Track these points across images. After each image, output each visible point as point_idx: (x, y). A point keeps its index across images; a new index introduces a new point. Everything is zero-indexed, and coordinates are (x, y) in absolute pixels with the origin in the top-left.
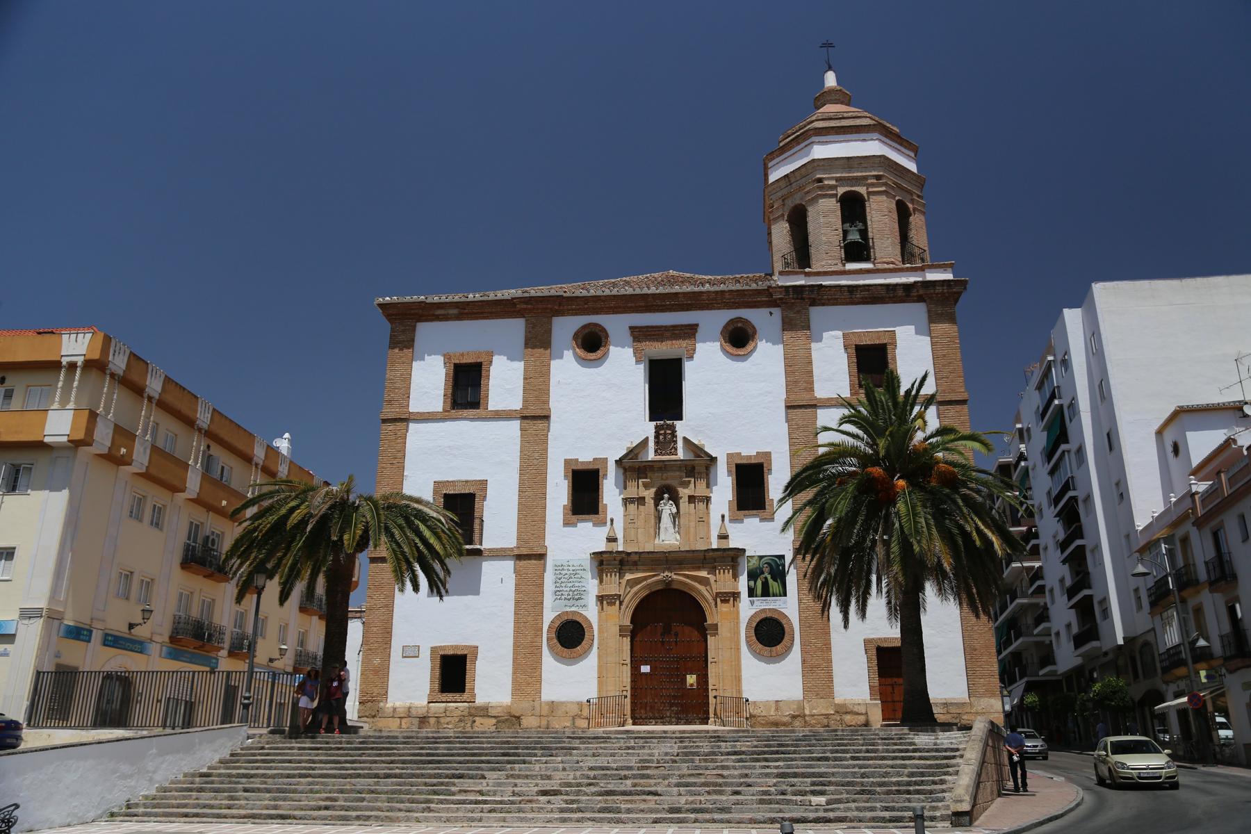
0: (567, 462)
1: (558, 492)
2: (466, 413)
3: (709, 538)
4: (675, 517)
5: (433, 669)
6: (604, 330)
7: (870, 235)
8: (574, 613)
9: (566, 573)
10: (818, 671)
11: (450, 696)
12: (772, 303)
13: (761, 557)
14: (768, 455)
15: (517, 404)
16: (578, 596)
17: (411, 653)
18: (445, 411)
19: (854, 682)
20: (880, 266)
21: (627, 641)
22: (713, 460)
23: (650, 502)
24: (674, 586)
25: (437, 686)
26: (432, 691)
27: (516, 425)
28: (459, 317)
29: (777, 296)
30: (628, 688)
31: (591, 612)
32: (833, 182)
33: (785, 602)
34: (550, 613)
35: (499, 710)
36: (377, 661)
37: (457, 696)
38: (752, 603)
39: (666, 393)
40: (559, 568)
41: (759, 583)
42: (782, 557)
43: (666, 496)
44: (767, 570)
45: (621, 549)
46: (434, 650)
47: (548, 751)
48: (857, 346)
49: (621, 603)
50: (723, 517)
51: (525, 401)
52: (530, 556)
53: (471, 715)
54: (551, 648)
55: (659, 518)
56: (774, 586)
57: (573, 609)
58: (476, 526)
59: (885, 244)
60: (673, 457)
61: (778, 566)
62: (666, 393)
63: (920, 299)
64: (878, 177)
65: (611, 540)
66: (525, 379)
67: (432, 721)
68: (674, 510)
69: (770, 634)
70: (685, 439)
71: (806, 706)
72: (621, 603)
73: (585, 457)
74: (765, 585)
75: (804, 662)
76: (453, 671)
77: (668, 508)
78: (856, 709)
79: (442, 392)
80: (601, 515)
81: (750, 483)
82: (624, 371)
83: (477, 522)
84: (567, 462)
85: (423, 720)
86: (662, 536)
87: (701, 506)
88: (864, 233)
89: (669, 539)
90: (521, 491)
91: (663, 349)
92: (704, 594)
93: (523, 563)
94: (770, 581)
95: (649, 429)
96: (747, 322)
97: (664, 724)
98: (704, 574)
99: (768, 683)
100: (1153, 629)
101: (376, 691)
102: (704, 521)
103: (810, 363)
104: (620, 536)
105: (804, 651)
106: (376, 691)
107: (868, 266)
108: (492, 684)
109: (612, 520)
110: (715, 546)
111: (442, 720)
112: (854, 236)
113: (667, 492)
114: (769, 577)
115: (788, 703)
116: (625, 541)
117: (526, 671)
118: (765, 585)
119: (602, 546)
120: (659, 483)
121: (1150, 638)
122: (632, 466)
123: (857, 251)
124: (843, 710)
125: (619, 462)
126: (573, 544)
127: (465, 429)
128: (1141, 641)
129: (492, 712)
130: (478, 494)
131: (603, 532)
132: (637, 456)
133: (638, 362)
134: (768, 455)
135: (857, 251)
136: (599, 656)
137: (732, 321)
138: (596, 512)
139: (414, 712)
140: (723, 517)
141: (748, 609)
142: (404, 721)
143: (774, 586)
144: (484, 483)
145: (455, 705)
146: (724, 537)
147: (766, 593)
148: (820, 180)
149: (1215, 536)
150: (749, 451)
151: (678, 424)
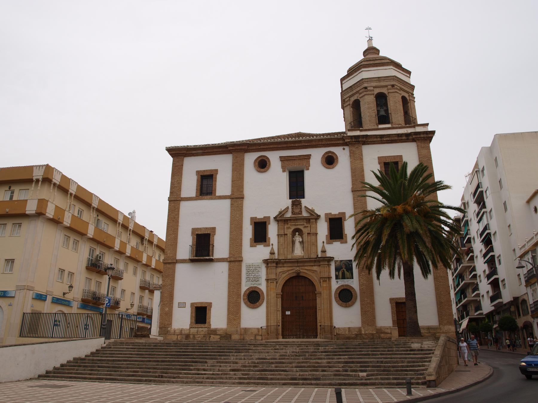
0: (252, 219)
1: (248, 232)
2: (206, 197)
3: (317, 252)
4: (302, 243)
5: (192, 313)
6: (268, 158)
7: (390, 112)
8: (256, 287)
9: (252, 269)
10: (368, 313)
11: (200, 325)
12: (346, 144)
13: (341, 261)
15: (228, 192)
16: (257, 279)
17: (182, 305)
18: (196, 196)
19: (385, 318)
20: (394, 126)
21: (280, 300)
22: (319, 216)
23: (290, 236)
24: (301, 274)
25: (194, 321)
26: (191, 323)
27: (228, 202)
28: (203, 154)
29: (347, 141)
30: (280, 322)
31: (263, 287)
32: (372, 88)
33: (353, 282)
34: (244, 287)
35: (222, 331)
36: (167, 309)
37: (202, 325)
38: (337, 282)
39: (297, 188)
40: (248, 267)
41: (340, 273)
43: (297, 233)
44: (344, 267)
45: (276, 258)
46: (192, 304)
47: (238, 351)
49: (277, 283)
50: (323, 242)
51: (232, 191)
52: (235, 260)
53: (209, 334)
54: (245, 303)
55: (293, 243)
56: (347, 274)
57: (255, 285)
58: (211, 248)
59: (397, 116)
60: (300, 215)
61: (349, 265)
62: (297, 188)
63: (414, 140)
64: (393, 86)
65: (272, 253)
66: (232, 181)
67: (191, 336)
68: (301, 240)
69: (346, 296)
70: (305, 207)
71: (362, 329)
72: (277, 283)
73: (260, 216)
74: (343, 274)
75: (362, 308)
76: (201, 313)
77: (298, 239)
78: (386, 331)
79: (195, 188)
80: (267, 242)
81: (336, 227)
82: (277, 179)
83: (211, 246)
84: (252, 219)
85: (187, 336)
86: (296, 252)
87: (313, 237)
88: (387, 111)
89: (298, 252)
90: (231, 232)
91: (296, 166)
92: (315, 278)
93: (233, 264)
94: (346, 272)
95: (289, 202)
96: (333, 153)
97: (297, 338)
98: (315, 268)
99: (346, 318)
100: (527, 293)
101: (166, 323)
102: (315, 244)
103: (363, 171)
104: (276, 251)
105: (362, 305)
106: (166, 323)
108: (218, 320)
109: (272, 245)
110: (319, 256)
111: (196, 336)
112: (383, 113)
113: (297, 231)
114: (345, 270)
115: (354, 328)
116: (278, 254)
117: (234, 313)
118: (343, 274)
119: (267, 256)
120: (293, 228)
121: (525, 297)
122: (280, 219)
124: (380, 331)
125: (275, 218)
126: (254, 255)
127: (206, 204)
128: (520, 300)
129: (218, 333)
130: (212, 233)
131: (268, 250)
132: (283, 215)
133: (284, 171)
136: (267, 307)
137: (327, 153)
138: (265, 241)
139: (183, 332)
140: (323, 242)
141: (335, 285)
142: (179, 336)
143: (347, 274)
144: (214, 229)
145: (202, 329)
146: (324, 251)
147: (344, 277)
148: (366, 88)
150: (335, 211)
151: (302, 200)
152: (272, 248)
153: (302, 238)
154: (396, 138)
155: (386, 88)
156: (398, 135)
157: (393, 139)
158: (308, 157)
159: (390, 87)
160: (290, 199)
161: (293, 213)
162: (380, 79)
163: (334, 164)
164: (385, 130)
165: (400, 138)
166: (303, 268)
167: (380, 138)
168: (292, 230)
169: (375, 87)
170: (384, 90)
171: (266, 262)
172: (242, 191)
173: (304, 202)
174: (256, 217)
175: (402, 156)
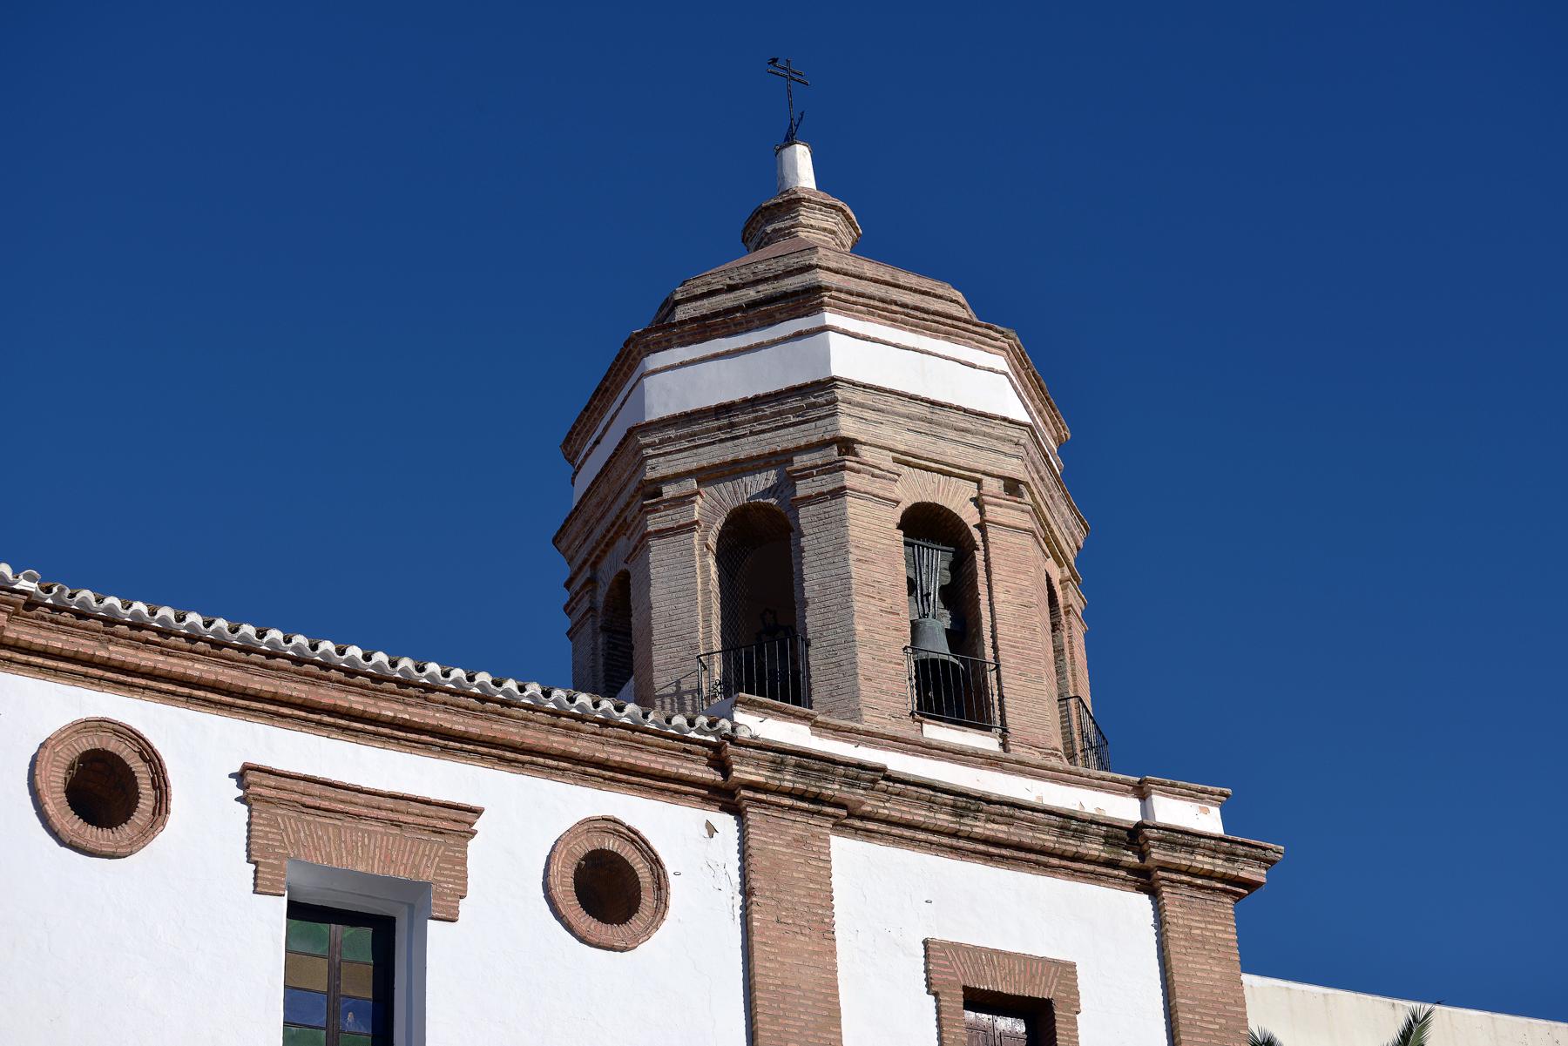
20: (1019, 752)
29: (744, 772)
32: (885, 460)
48: (965, 988)
63: (1145, 881)
103: (833, 1016)
107: (987, 742)
123: (954, 687)
135: (954, 687)
137: (592, 825)
154: (1049, 840)
155: (971, 489)
156: (1068, 822)
157: (1027, 837)
158: (459, 820)
159: (993, 486)
162: (940, 415)
163: (636, 923)
164: (950, 759)
165: (1071, 846)
167: (958, 812)
169: (908, 460)
170: (957, 499)
175: (1073, 965)
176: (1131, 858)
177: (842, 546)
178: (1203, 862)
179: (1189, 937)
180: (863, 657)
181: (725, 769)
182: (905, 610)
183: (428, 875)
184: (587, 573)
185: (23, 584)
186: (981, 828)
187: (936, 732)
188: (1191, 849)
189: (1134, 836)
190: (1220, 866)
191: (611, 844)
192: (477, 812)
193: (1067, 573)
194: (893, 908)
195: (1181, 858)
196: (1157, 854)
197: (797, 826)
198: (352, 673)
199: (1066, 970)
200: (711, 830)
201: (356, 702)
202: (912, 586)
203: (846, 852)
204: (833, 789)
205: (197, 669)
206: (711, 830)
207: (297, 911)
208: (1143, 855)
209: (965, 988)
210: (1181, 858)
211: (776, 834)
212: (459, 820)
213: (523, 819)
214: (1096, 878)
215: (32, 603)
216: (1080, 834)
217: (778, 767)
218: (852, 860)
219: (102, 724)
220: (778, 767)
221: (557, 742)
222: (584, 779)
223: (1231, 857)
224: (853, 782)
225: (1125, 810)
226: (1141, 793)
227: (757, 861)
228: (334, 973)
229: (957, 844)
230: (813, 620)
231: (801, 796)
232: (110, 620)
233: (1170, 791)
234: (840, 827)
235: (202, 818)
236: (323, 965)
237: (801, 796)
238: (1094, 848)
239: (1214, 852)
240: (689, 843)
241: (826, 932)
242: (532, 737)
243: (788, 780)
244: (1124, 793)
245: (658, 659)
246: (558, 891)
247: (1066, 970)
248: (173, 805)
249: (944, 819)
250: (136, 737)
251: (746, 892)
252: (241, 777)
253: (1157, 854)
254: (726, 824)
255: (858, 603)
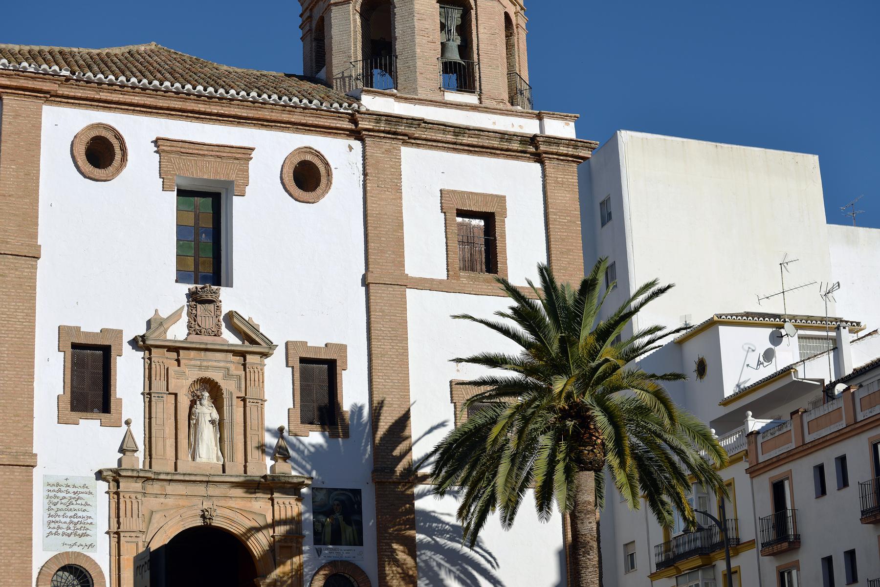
4: (219, 425)
8: (79, 554)
9: (66, 496)
13: (330, 491)
14: (343, 348)
16: (81, 528)
20: (487, 103)
22: (271, 346)
23: (184, 402)
29: (363, 124)
38: (319, 552)
40: (54, 487)
42: (357, 492)
48: (457, 210)
56: (348, 532)
57: (76, 549)
59: (491, 71)
63: (538, 158)
68: (216, 416)
73: (91, 325)
77: (207, 411)
96: (318, 155)
103: (400, 226)
109: (128, 423)
114: (340, 518)
123: (461, 74)
134: (343, 348)
135: (461, 74)
143: (348, 532)
147: (336, 540)
149: (778, 489)
150: (316, 340)
152: (128, 435)
153: (220, 410)
154: (496, 143)
156: (504, 136)
157: (486, 143)
158: (246, 153)
160: (181, 278)
161: (194, 327)
163: (319, 190)
165: (505, 145)
166: (222, 503)
167: (456, 134)
168: (190, 381)
171: (113, 477)
172: (35, 236)
173: (228, 299)
174: (78, 329)
175: (505, 197)
176: (532, 149)
177: (411, 13)
178: (563, 150)
179: (557, 182)
180: (419, 63)
181: (356, 123)
182: (438, 37)
183: (233, 177)
184: (307, 14)
185: (64, 73)
186: (466, 140)
187: (452, 96)
188: (558, 144)
189: (533, 140)
190: (571, 151)
191: (309, 158)
192: (253, 149)
193: (519, 8)
194: (427, 176)
195: (554, 149)
196: (543, 148)
197: (387, 144)
198: (199, 96)
199: (502, 199)
200: (351, 148)
201: (202, 107)
202: (443, 26)
203: (408, 153)
204: (401, 129)
205: (136, 99)
206: (351, 148)
207: (181, 193)
208: (537, 148)
209: (457, 210)
210: (554, 149)
211: (378, 148)
212: (246, 153)
213: (272, 150)
214: (517, 158)
215: (68, 79)
216: (509, 140)
217: (378, 121)
218: (411, 158)
219: (99, 125)
220: (378, 121)
221: (285, 117)
222: (297, 131)
223: (576, 147)
224: (410, 125)
225: (530, 127)
226: (540, 117)
227: (370, 161)
228: (197, 218)
229: (456, 147)
230: (399, 46)
231: (388, 132)
232: (100, 83)
233: (552, 116)
234: (405, 143)
235: (141, 162)
236: (192, 215)
237: (388, 132)
238: (515, 146)
239: (568, 145)
240: (341, 155)
241: (398, 189)
242: (275, 116)
243: (383, 126)
244: (532, 118)
245: (335, 61)
246: (286, 181)
247: (502, 199)
248: (129, 158)
249: (450, 137)
250: (113, 130)
251: (365, 174)
252: (156, 142)
253: (543, 148)
254: (357, 145)
255: (418, 39)
